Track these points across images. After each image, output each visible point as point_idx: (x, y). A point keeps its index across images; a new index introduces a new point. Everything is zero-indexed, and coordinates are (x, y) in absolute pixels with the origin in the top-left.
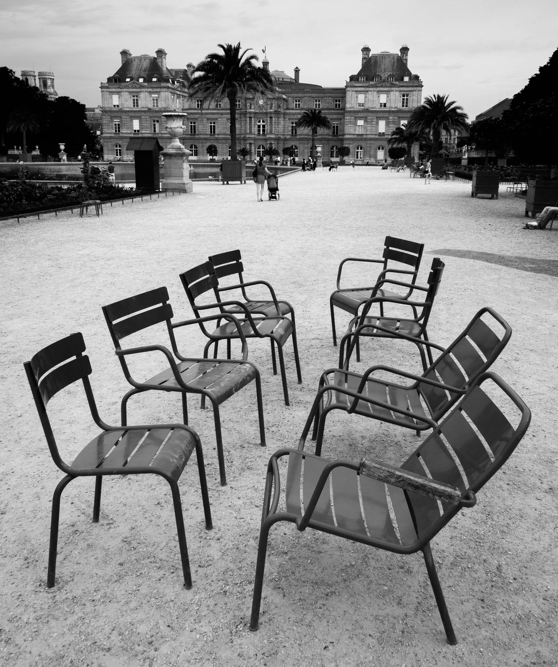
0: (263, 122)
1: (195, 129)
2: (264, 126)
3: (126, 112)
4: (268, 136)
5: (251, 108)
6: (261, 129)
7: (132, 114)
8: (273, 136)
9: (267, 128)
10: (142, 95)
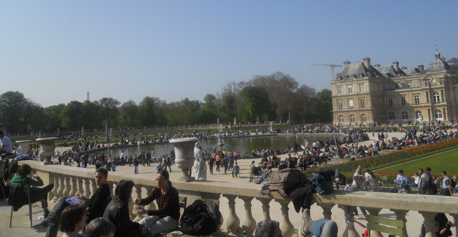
0: (437, 94)
1: (392, 102)
2: (438, 97)
3: (344, 96)
4: (441, 104)
5: (426, 86)
6: (437, 99)
7: (348, 97)
8: (445, 103)
9: (440, 98)
10: (353, 85)
